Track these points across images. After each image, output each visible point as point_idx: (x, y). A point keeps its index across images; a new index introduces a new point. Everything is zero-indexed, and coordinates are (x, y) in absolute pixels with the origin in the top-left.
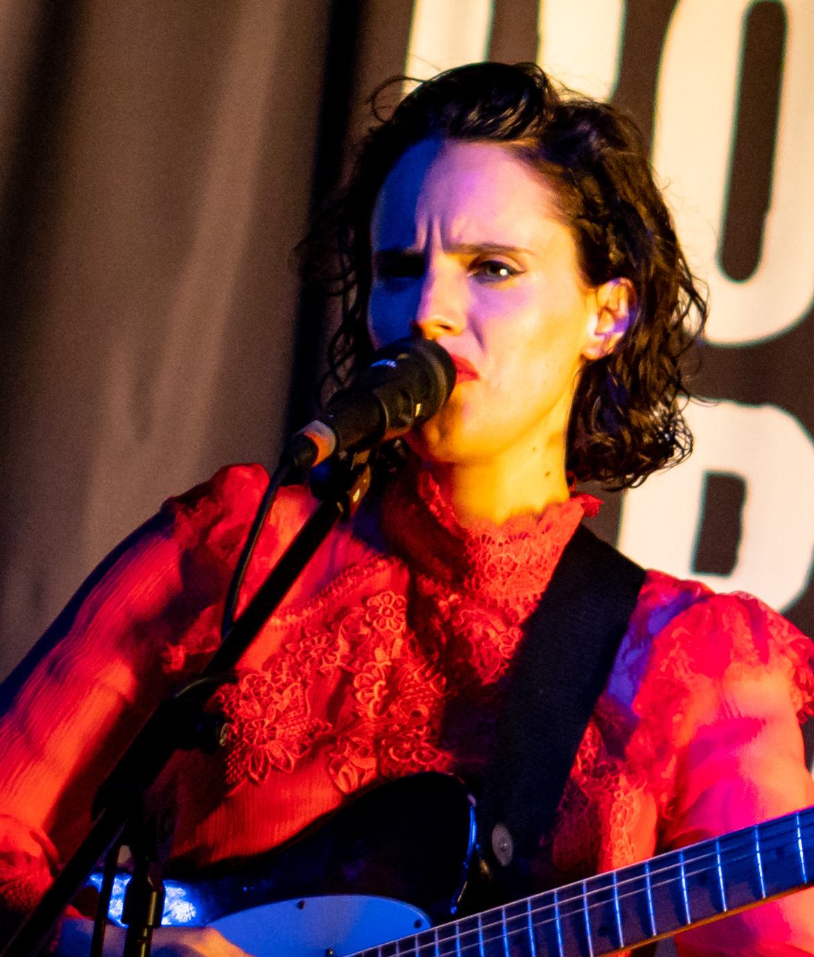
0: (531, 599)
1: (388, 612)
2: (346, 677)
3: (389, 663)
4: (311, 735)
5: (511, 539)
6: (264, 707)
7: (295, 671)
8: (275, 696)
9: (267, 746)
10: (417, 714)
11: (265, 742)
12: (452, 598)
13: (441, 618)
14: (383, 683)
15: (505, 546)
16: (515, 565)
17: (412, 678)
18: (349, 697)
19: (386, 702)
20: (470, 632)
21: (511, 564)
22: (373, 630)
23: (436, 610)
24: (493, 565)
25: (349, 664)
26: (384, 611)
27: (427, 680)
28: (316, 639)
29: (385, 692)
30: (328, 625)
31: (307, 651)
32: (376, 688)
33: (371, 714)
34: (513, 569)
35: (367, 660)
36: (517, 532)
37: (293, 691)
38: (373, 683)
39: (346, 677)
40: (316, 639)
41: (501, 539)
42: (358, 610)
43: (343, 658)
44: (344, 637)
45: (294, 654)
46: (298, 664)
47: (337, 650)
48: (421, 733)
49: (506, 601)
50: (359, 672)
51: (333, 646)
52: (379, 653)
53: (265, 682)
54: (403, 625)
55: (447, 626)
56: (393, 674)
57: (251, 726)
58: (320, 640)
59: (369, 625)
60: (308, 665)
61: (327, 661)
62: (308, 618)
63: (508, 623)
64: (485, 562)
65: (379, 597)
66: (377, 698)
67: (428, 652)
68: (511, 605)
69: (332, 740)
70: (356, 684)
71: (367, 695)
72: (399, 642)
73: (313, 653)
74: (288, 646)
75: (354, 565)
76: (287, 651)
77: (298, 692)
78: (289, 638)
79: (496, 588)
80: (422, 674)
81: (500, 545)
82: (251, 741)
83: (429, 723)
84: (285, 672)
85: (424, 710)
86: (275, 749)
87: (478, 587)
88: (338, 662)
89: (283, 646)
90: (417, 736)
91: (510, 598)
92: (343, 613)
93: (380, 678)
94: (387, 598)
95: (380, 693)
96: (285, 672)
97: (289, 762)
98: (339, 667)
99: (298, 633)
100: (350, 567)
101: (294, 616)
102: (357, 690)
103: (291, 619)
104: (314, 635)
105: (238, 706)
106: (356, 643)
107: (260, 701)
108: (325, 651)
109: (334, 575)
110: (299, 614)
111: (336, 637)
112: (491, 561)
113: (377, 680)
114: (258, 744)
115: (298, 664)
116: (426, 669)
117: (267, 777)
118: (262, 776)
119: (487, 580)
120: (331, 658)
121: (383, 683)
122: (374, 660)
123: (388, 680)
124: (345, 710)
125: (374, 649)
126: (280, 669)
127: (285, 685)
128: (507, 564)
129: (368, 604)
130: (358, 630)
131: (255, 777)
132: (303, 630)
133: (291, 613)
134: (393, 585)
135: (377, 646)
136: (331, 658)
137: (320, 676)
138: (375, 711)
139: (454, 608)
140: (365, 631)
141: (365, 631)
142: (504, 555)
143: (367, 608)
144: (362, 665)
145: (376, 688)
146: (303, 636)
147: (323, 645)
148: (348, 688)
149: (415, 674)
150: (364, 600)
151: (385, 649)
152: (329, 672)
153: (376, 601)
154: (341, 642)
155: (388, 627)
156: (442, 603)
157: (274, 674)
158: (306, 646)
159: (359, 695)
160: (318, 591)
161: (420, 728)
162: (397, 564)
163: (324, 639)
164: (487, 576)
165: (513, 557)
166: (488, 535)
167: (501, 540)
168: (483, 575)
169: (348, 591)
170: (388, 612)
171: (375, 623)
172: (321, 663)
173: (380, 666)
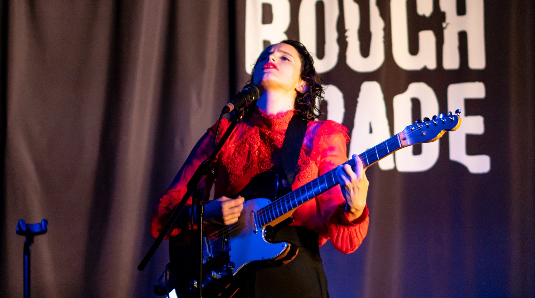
0: (285, 129)
2: (250, 152)
4: (245, 167)
8: (236, 160)
9: (236, 172)
10: (265, 156)
11: (236, 171)
12: (269, 132)
14: (257, 151)
17: (263, 150)
18: (251, 156)
19: (259, 155)
20: (273, 137)
23: (266, 135)
24: (275, 123)
27: (266, 149)
29: (258, 153)
31: (240, 149)
32: (256, 152)
33: (256, 158)
34: (280, 123)
35: (253, 148)
39: (250, 152)
42: (249, 139)
44: (247, 144)
45: (238, 150)
48: (267, 160)
49: (280, 130)
51: (245, 146)
52: (255, 146)
54: (259, 139)
56: (259, 149)
57: (232, 169)
59: (252, 141)
60: (241, 151)
63: (281, 134)
64: (274, 123)
66: (257, 155)
67: (266, 144)
68: (281, 131)
69: (249, 167)
70: (252, 153)
72: (259, 143)
74: (236, 149)
79: (277, 128)
80: (265, 148)
81: (276, 119)
82: (233, 172)
83: (268, 158)
85: (267, 155)
86: (238, 172)
87: (273, 128)
90: (266, 161)
92: (246, 139)
93: (257, 150)
94: (255, 135)
97: (241, 174)
98: (248, 150)
102: (252, 154)
105: (229, 165)
106: (250, 145)
108: (244, 148)
112: (275, 122)
113: (256, 151)
114: (234, 172)
116: (266, 147)
117: (238, 178)
118: (237, 178)
119: (275, 127)
120: (245, 149)
121: (257, 151)
123: (258, 151)
131: (235, 179)
134: (256, 132)
138: (257, 157)
139: (269, 134)
140: (251, 142)
141: (251, 142)
143: (251, 138)
144: (252, 149)
149: (264, 148)
150: (250, 136)
151: (256, 144)
155: (256, 140)
156: (267, 133)
159: (253, 155)
161: (267, 159)
163: (243, 146)
164: (275, 126)
167: (276, 118)
168: (274, 126)
172: (244, 150)
173: (256, 148)
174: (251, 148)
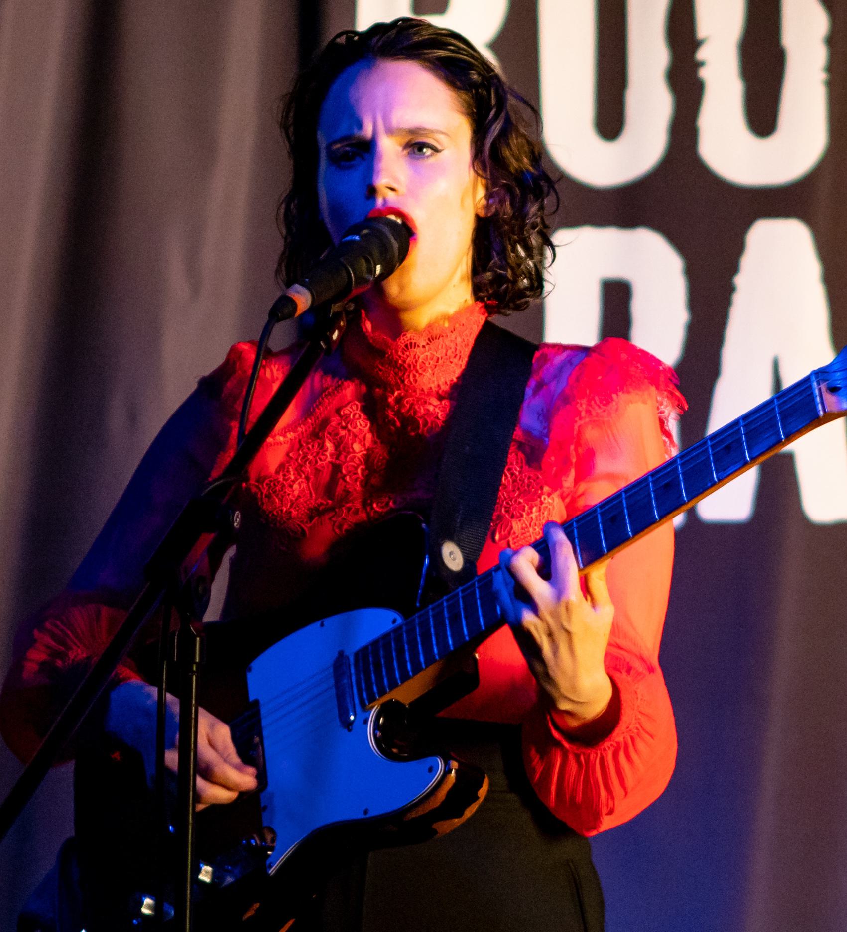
1: (357, 416)
3: (365, 452)
5: (431, 340)
6: (281, 500)
7: (299, 470)
13: (392, 409)
15: (427, 347)
16: (438, 359)
20: (415, 412)
21: (435, 359)
22: (349, 431)
25: (337, 458)
26: (354, 416)
28: (310, 446)
30: (317, 435)
34: (437, 362)
35: (349, 453)
36: (432, 335)
37: (300, 484)
38: (356, 468)
40: (310, 446)
41: (422, 343)
43: (331, 455)
45: (297, 460)
46: (300, 466)
47: (326, 451)
50: (344, 463)
51: (322, 447)
52: (356, 447)
53: (279, 481)
55: (398, 413)
58: (313, 446)
61: (321, 460)
62: (302, 433)
64: (416, 362)
65: (348, 408)
70: (344, 471)
71: (354, 477)
72: (369, 436)
73: (310, 457)
74: (291, 455)
75: (327, 388)
76: (291, 458)
77: (304, 485)
78: (291, 449)
81: (424, 347)
84: (292, 473)
87: (416, 381)
88: (329, 459)
89: (287, 454)
91: (440, 383)
92: (325, 422)
93: (361, 464)
94: (354, 407)
95: (362, 474)
96: (292, 473)
98: (330, 462)
99: (297, 446)
100: (324, 391)
101: (292, 433)
102: (345, 476)
103: (290, 435)
104: (308, 444)
107: (277, 496)
108: (318, 453)
109: (315, 398)
110: (295, 431)
111: (324, 442)
112: (420, 360)
113: (358, 466)
115: (300, 466)
120: (322, 457)
122: (354, 452)
124: (339, 490)
125: (352, 444)
126: (289, 472)
127: (294, 481)
128: (432, 359)
129: (342, 413)
130: (337, 434)
132: (300, 442)
133: (289, 431)
135: (353, 442)
136: (322, 457)
137: (317, 471)
141: (343, 433)
142: (428, 354)
144: (346, 457)
145: (359, 471)
146: (301, 446)
147: (316, 450)
148: (339, 475)
150: (338, 411)
151: (360, 443)
152: (323, 467)
153: (347, 410)
154: (329, 445)
157: (284, 475)
158: (304, 453)
159: (348, 479)
160: (306, 412)
162: (357, 381)
163: (316, 445)
165: (435, 353)
166: (413, 342)
168: (417, 371)
169: (326, 407)
170: (357, 416)
171: (349, 427)
172: (317, 462)
173: (359, 455)
174: (342, 457)
